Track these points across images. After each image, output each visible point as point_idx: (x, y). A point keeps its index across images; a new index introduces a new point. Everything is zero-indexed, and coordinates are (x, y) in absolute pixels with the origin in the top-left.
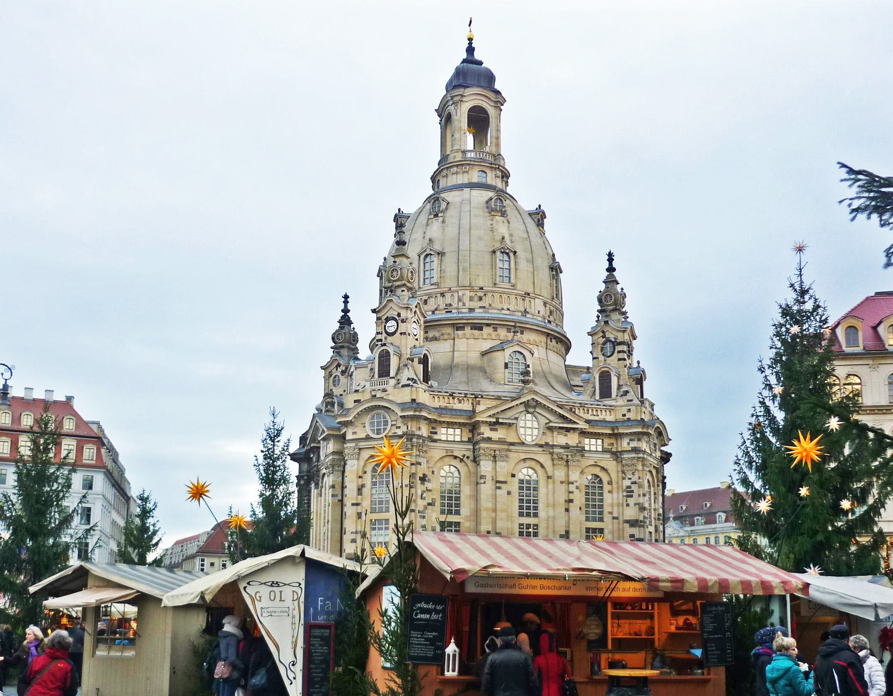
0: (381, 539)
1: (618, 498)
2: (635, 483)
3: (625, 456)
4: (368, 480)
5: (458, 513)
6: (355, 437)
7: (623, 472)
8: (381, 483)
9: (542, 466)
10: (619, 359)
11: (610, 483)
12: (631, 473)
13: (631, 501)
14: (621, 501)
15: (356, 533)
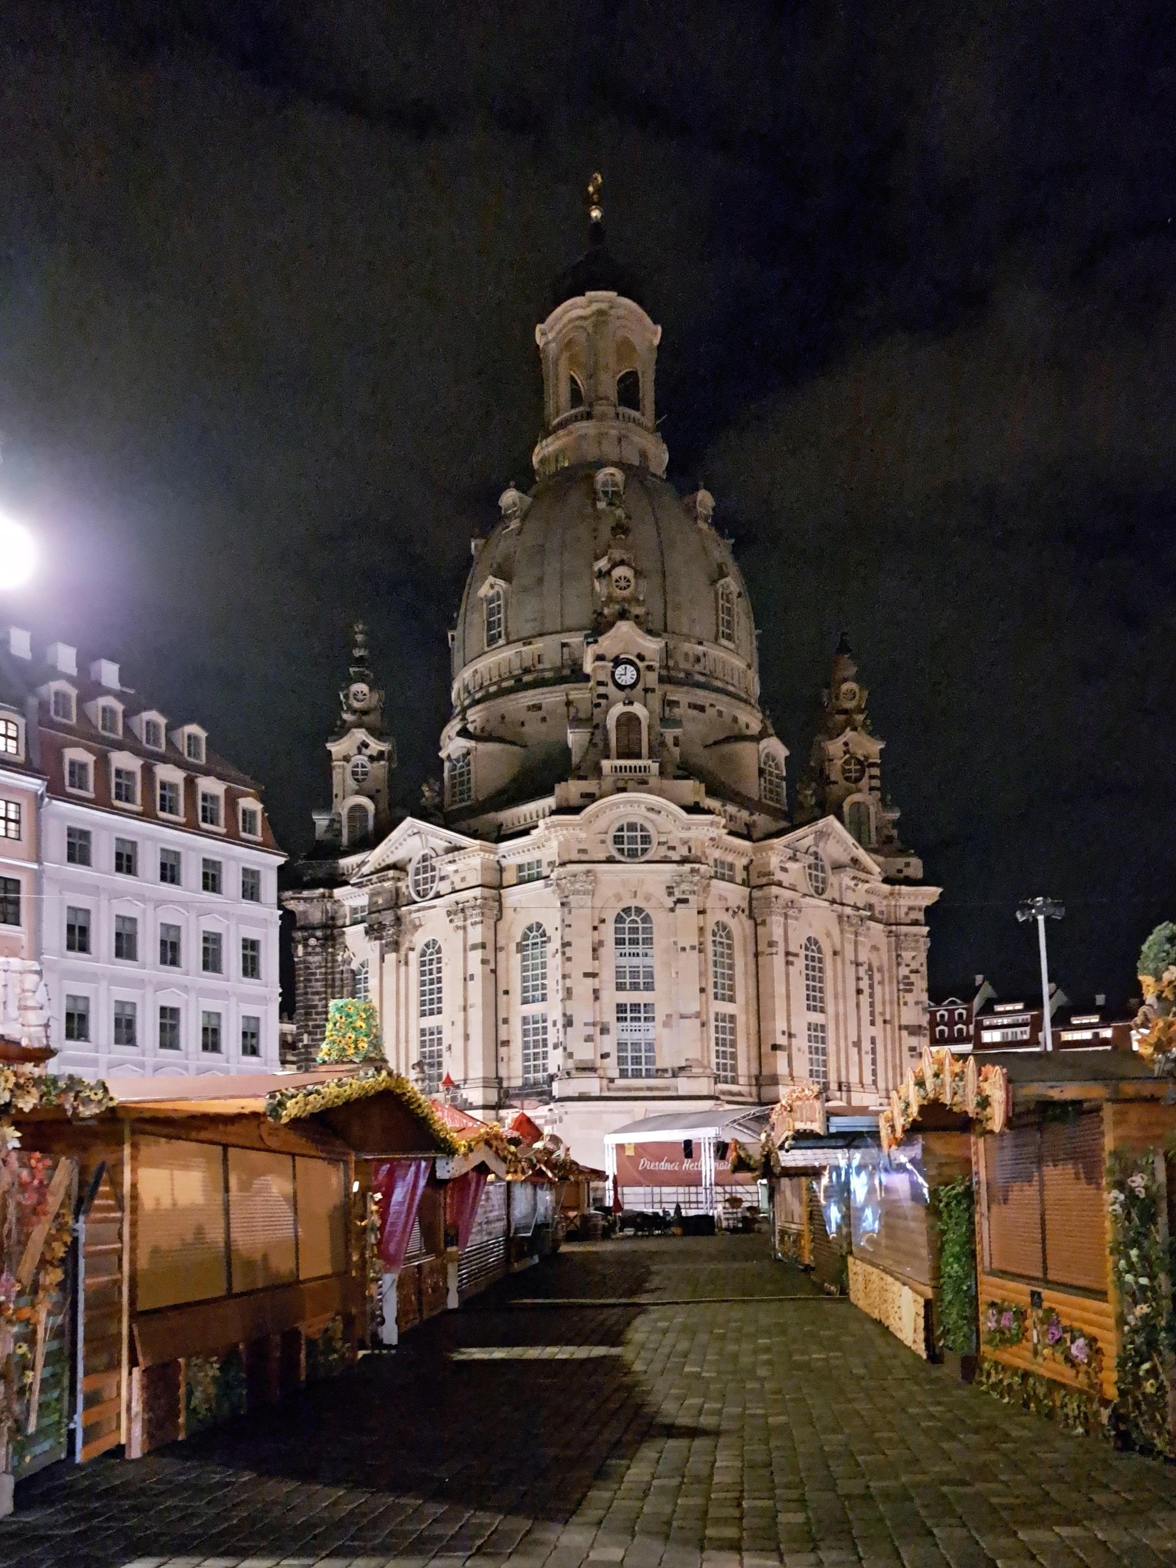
1: (891, 993)
2: (917, 972)
3: (904, 929)
4: (608, 933)
6: (584, 857)
7: (898, 956)
8: (634, 942)
9: (828, 935)
11: (880, 970)
13: (910, 998)
14: (896, 998)
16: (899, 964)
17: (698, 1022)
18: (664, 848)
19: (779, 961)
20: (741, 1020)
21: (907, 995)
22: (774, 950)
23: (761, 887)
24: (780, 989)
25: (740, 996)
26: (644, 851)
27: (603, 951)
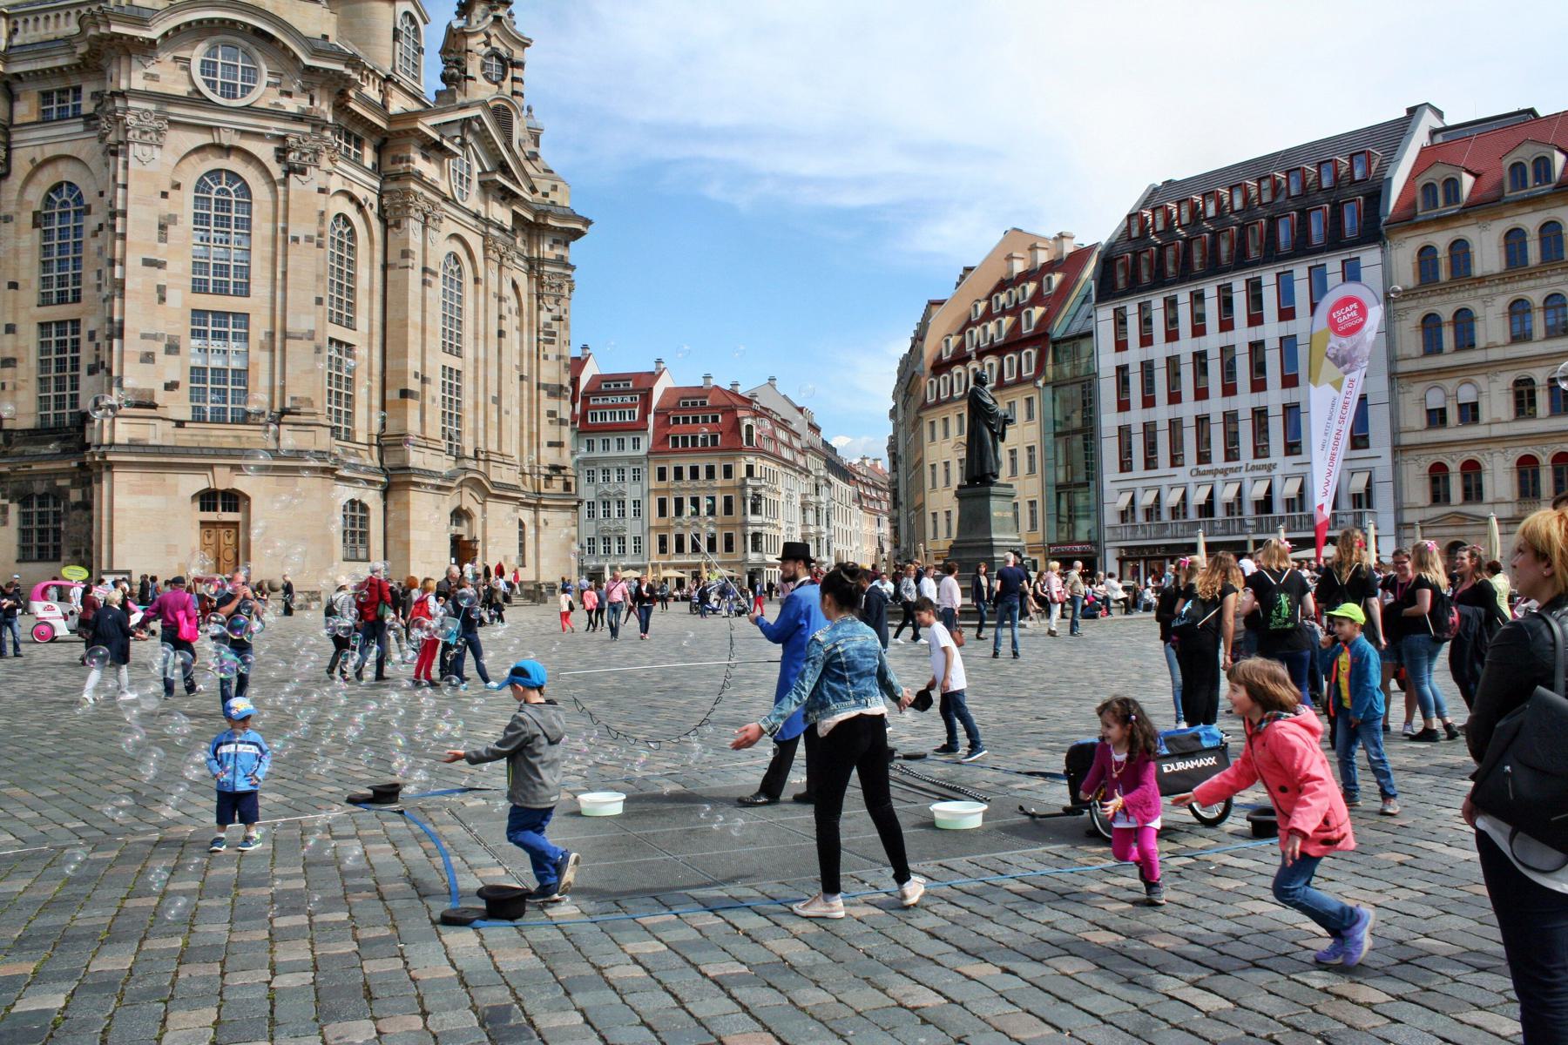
0: (216, 362)
1: (530, 343)
2: (560, 319)
5: (351, 325)
6: (153, 87)
8: (223, 222)
10: (514, 93)
12: (552, 299)
13: (551, 351)
15: (154, 337)
16: (539, 308)
17: (311, 345)
18: (275, 92)
19: (415, 276)
20: (361, 351)
22: (410, 262)
23: (397, 177)
24: (414, 316)
25: (362, 321)
26: (247, 90)
27: (171, 229)
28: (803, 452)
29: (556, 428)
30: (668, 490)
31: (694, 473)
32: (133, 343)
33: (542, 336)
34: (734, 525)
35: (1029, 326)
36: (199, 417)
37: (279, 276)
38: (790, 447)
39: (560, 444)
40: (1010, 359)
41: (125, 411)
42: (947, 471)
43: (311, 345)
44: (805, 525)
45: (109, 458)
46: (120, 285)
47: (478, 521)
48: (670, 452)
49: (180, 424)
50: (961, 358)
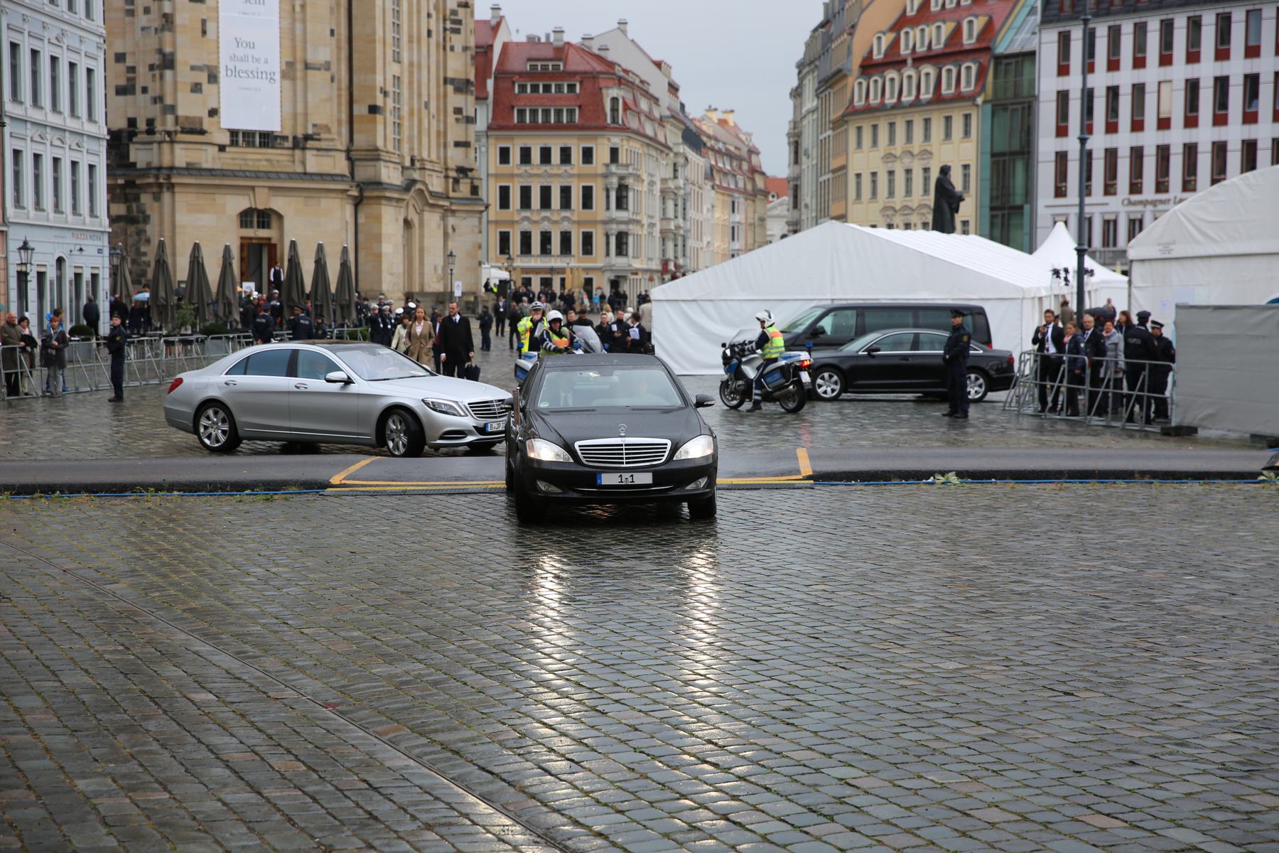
2: (466, 5)
13: (457, 41)
17: (327, 75)
21: (454, 37)
28: (661, 121)
29: (462, 126)
30: (512, 176)
31: (546, 155)
32: (184, 74)
33: (449, 25)
34: (595, 223)
35: (970, 36)
36: (234, 143)
37: (298, 9)
38: (650, 117)
39: (466, 144)
40: (949, 71)
41: (180, 137)
42: (874, 182)
43: (327, 75)
44: (664, 218)
45: (174, 180)
46: (168, 21)
47: (416, 230)
48: (515, 128)
49: (222, 148)
50: (893, 61)
